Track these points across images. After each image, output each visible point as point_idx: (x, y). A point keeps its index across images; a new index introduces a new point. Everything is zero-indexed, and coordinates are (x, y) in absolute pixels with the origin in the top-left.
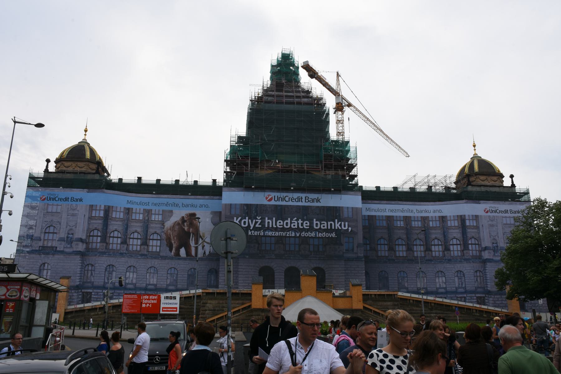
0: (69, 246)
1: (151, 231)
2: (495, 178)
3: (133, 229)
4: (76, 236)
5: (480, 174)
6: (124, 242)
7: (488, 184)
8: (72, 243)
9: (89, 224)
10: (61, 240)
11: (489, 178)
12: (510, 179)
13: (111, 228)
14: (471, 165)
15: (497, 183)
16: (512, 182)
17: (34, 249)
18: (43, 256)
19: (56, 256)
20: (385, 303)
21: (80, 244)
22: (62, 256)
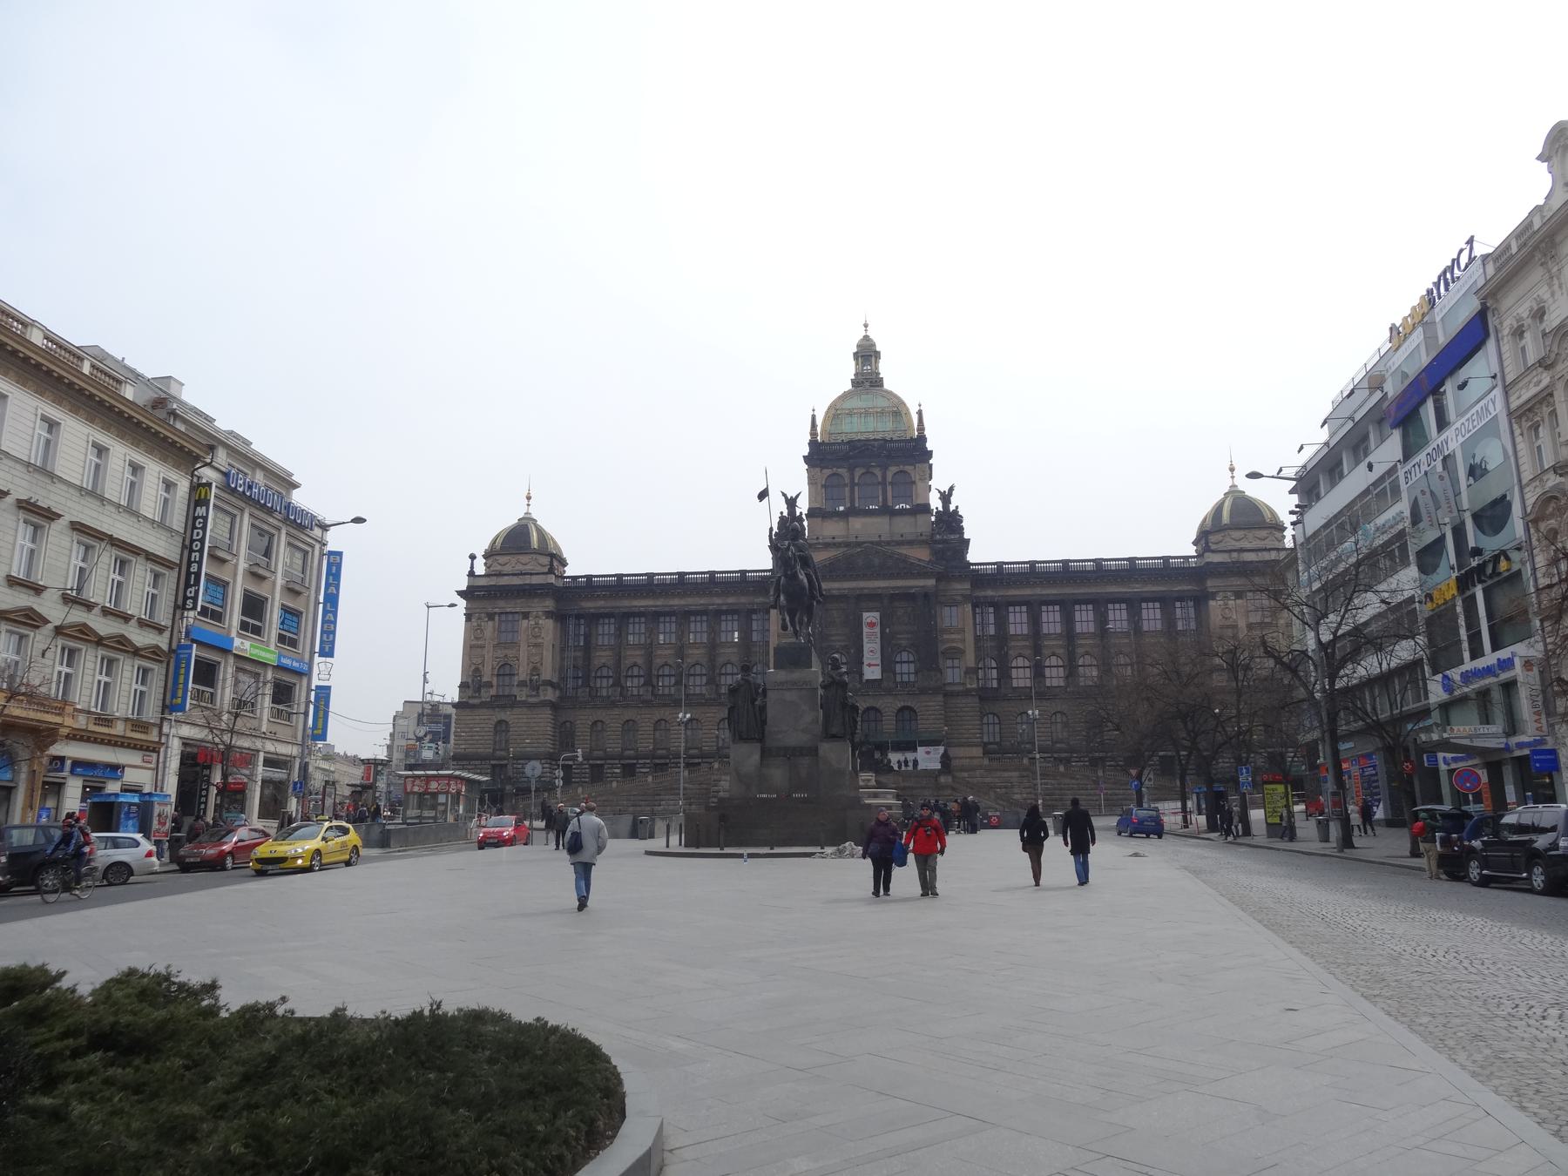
1: (658, 661)
2: (1264, 533)
3: (629, 662)
4: (544, 677)
5: (1234, 526)
6: (617, 683)
7: (1249, 546)
9: (562, 659)
10: (522, 684)
11: (1250, 535)
13: (596, 662)
14: (1218, 510)
15: (1269, 544)
19: (516, 711)
20: (1006, 774)
21: (550, 689)
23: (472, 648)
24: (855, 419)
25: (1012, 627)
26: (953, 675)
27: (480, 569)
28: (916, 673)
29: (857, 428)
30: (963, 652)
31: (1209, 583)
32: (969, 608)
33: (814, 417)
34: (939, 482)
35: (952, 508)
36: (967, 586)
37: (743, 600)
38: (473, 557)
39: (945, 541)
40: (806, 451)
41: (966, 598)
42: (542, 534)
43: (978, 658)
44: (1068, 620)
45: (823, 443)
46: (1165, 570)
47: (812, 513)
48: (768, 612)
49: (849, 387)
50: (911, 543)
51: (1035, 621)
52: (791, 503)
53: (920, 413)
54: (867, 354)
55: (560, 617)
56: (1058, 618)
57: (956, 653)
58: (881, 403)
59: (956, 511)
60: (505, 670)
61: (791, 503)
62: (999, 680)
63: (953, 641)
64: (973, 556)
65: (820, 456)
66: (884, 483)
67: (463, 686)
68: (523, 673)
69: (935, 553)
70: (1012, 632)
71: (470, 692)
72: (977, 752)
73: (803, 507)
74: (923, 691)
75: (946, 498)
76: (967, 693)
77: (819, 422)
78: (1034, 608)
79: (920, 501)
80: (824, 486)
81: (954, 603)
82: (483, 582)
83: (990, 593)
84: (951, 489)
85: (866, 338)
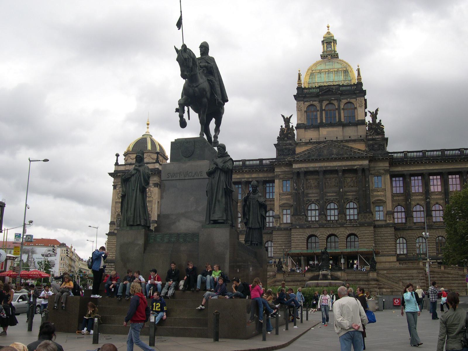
4: (152, 219)
20: (410, 271)
24: (323, 75)
25: (413, 188)
26: (379, 216)
27: (122, 161)
28: (358, 214)
29: (323, 80)
32: (388, 177)
33: (299, 75)
34: (371, 108)
35: (378, 121)
37: (261, 175)
38: (117, 155)
39: (373, 139)
40: (295, 92)
41: (387, 171)
42: (153, 142)
43: (394, 207)
44: (445, 184)
45: (305, 88)
47: (298, 127)
49: (319, 59)
50: (354, 141)
51: (426, 185)
52: (287, 121)
53: (358, 70)
54: (329, 41)
56: (439, 183)
57: (382, 203)
58: (337, 66)
59: (380, 123)
61: (287, 121)
62: (406, 218)
63: (378, 196)
64: (390, 148)
65: (302, 94)
66: (339, 109)
67: (112, 223)
69: (368, 146)
70: (413, 191)
71: (115, 227)
72: (394, 259)
73: (294, 122)
74: (362, 225)
75: (374, 116)
76: (387, 226)
77: (302, 78)
78: (425, 177)
79: (360, 118)
80: (306, 112)
81: (379, 175)
82: (122, 168)
83: (399, 169)
84: (377, 110)
85: (329, 33)
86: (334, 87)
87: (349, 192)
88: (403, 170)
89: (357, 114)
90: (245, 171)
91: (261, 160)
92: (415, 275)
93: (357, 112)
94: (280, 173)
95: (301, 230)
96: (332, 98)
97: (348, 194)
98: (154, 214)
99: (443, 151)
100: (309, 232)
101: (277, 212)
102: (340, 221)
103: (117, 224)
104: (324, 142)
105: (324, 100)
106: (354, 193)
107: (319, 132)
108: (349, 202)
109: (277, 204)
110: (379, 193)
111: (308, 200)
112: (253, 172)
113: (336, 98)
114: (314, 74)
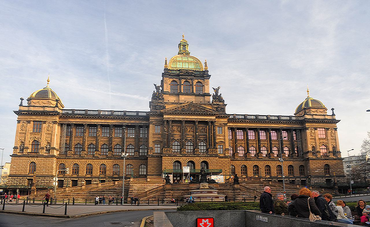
0: (47, 152)
2: (322, 110)
7: (317, 114)
8: (49, 150)
9: (61, 140)
10: (43, 148)
12: (332, 111)
14: (307, 103)
16: (333, 112)
17: (24, 154)
18: (30, 158)
20: (254, 185)
22: (43, 158)
23: (22, 133)
28: (207, 150)
30: (224, 143)
31: (307, 124)
32: (226, 128)
33: (166, 61)
36: (226, 120)
37: (137, 122)
46: (290, 120)
48: (148, 127)
55: (61, 125)
60: (36, 143)
66: (192, 85)
67: (15, 148)
68: (44, 144)
81: (220, 126)
86: (190, 71)
87: (202, 135)
88: (232, 125)
89: (205, 89)
90: (126, 118)
91: (138, 112)
92: (257, 187)
93: (205, 88)
94: (153, 121)
95: (169, 157)
96: (189, 78)
97: (200, 136)
98: (54, 143)
99: (256, 116)
100: (175, 159)
101: (151, 145)
102: (196, 153)
103: (20, 148)
104: (184, 103)
105: (182, 79)
106: (204, 136)
107: (179, 98)
108: (201, 142)
109: (151, 140)
110: (221, 137)
111: (173, 139)
112: (132, 119)
113: (191, 78)
114: (175, 62)
